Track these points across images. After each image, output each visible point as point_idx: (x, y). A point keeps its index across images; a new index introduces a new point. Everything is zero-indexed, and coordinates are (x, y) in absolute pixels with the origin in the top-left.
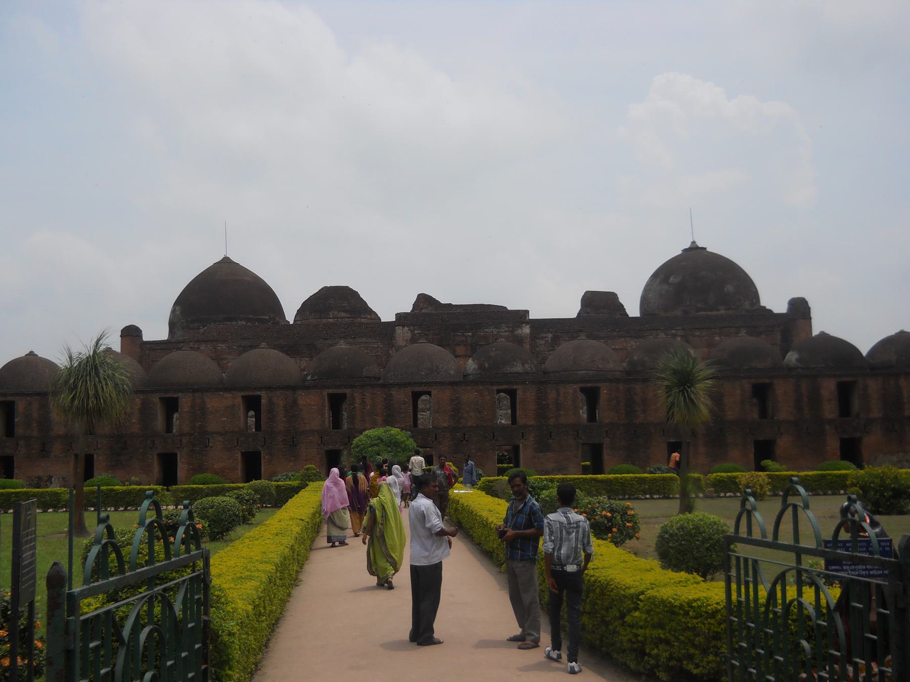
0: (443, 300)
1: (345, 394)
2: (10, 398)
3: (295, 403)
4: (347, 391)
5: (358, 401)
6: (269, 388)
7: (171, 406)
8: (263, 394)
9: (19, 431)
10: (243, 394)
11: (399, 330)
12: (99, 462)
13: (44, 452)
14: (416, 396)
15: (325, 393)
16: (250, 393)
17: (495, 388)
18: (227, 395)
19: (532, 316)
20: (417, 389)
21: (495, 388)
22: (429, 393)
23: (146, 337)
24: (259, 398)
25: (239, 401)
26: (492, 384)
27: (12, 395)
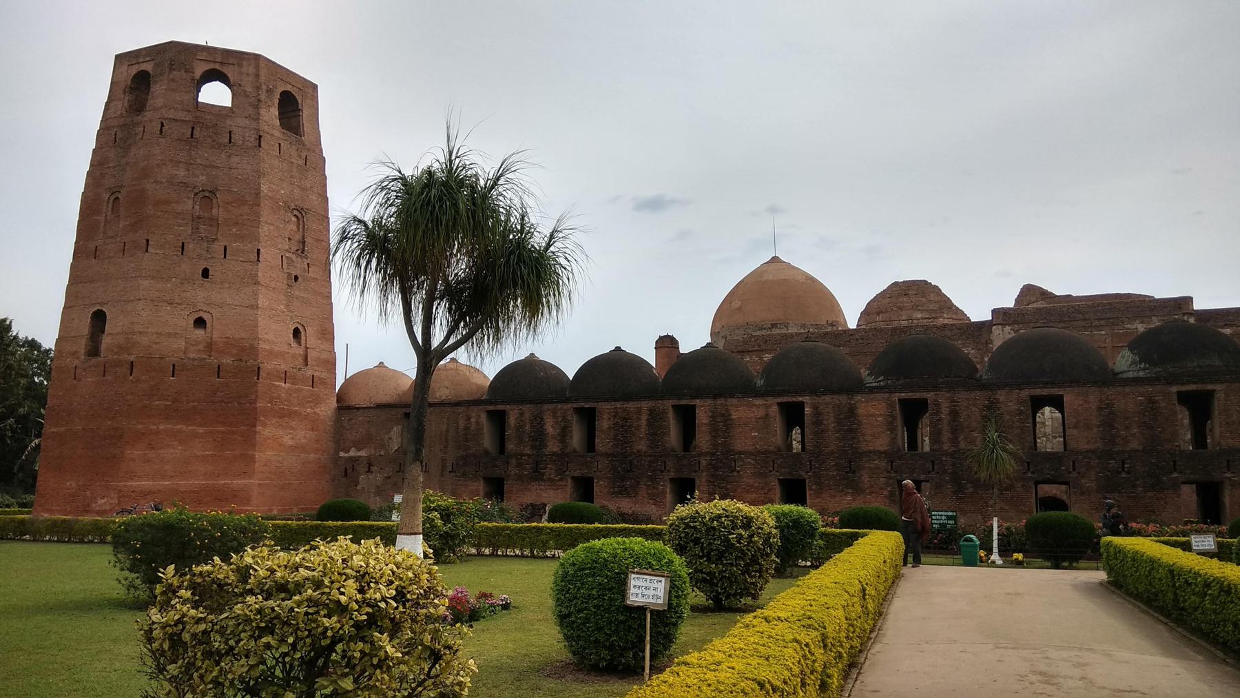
0: (1058, 291)
1: (925, 400)
2: (500, 407)
3: (852, 411)
4: (929, 396)
5: (945, 410)
6: (813, 392)
7: (687, 417)
8: (806, 399)
9: (510, 447)
10: (779, 400)
11: (996, 330)
12: (599, 488)
13: (537, 475)
14: (1037, 404)
15: (896, 397)
16: (790, 399)
17: (1174, 389)
18: (759, 402)
19: (1197, 306)
20: (1038, 392)
21: (1174, 389)
22: (1057, 403)
23: (685, 347)
24: (802, 405)
25: (774, 410)
26: (1170, 383)
27: (503, 403)
